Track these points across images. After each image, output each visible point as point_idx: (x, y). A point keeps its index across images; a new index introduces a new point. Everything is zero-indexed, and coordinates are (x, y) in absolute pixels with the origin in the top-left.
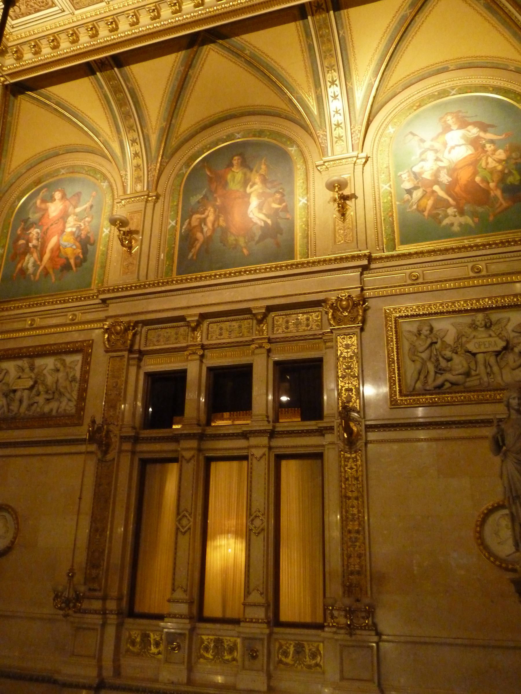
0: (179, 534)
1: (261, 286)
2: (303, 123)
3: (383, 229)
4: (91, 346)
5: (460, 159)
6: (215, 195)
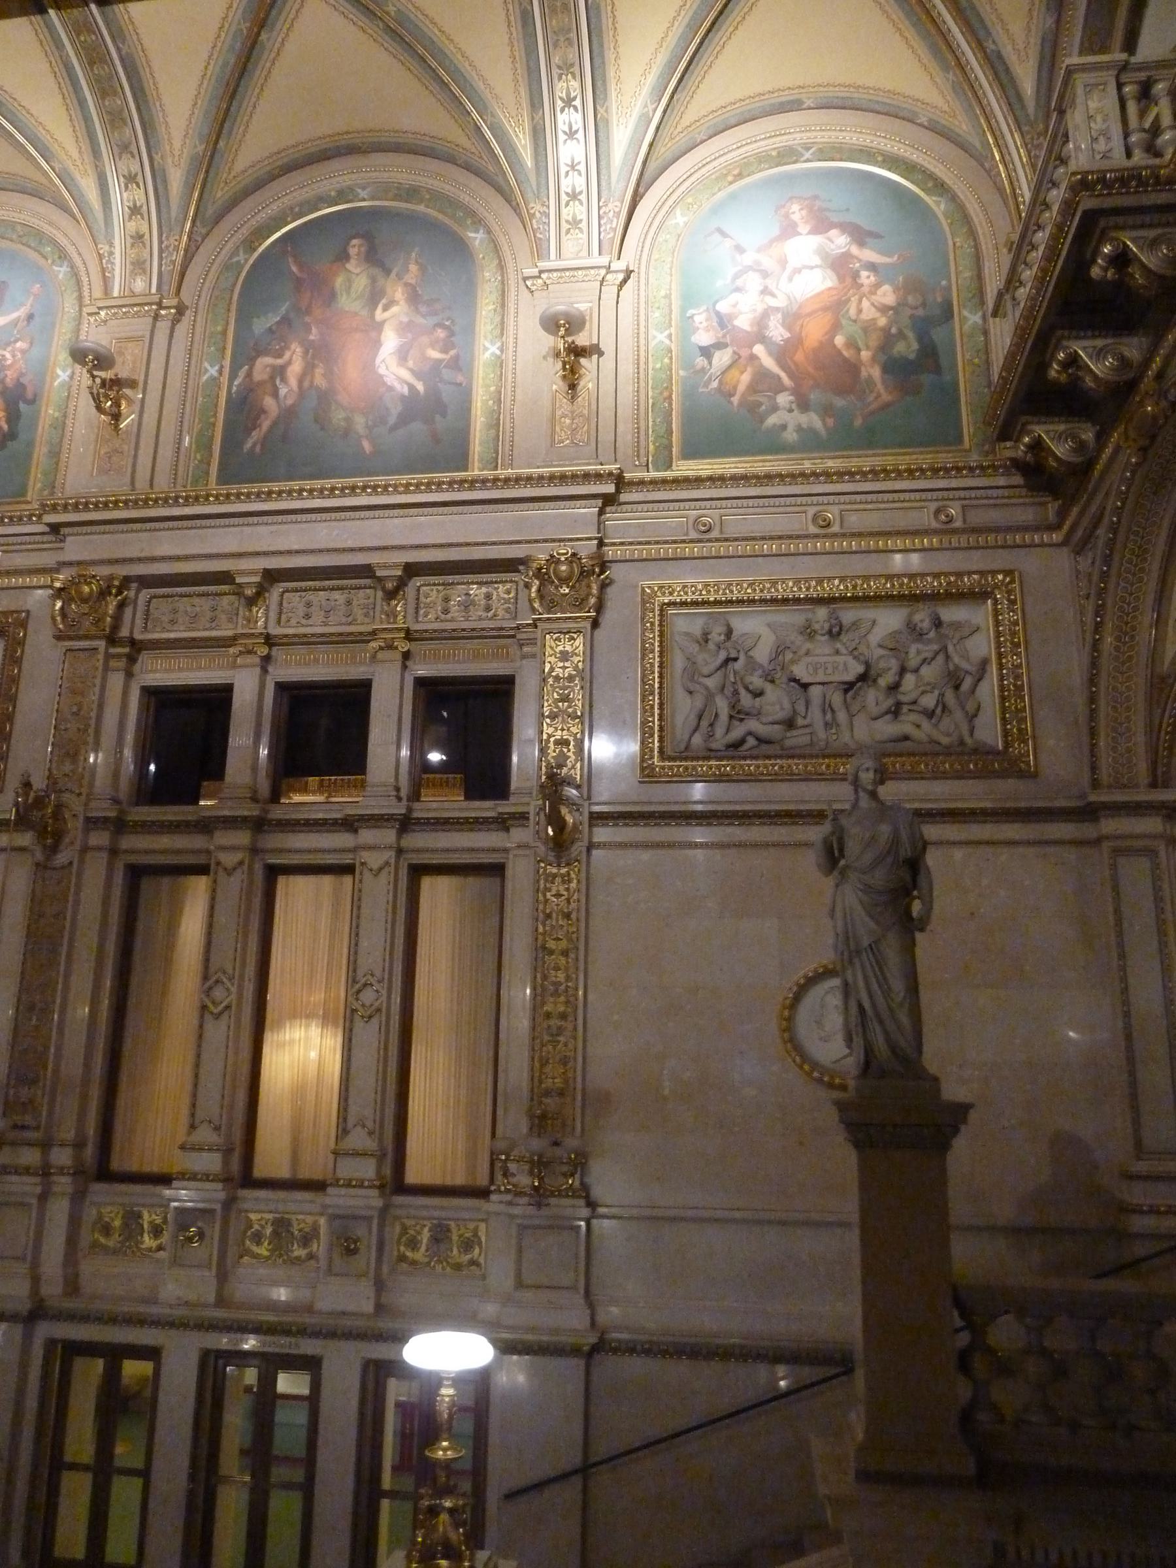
0: (207, 1016)
1: (396, 521)
2: (500, 179)
3: (651, 424)
4: (23, 624)
5: (809, 296)
6: (307, 319)
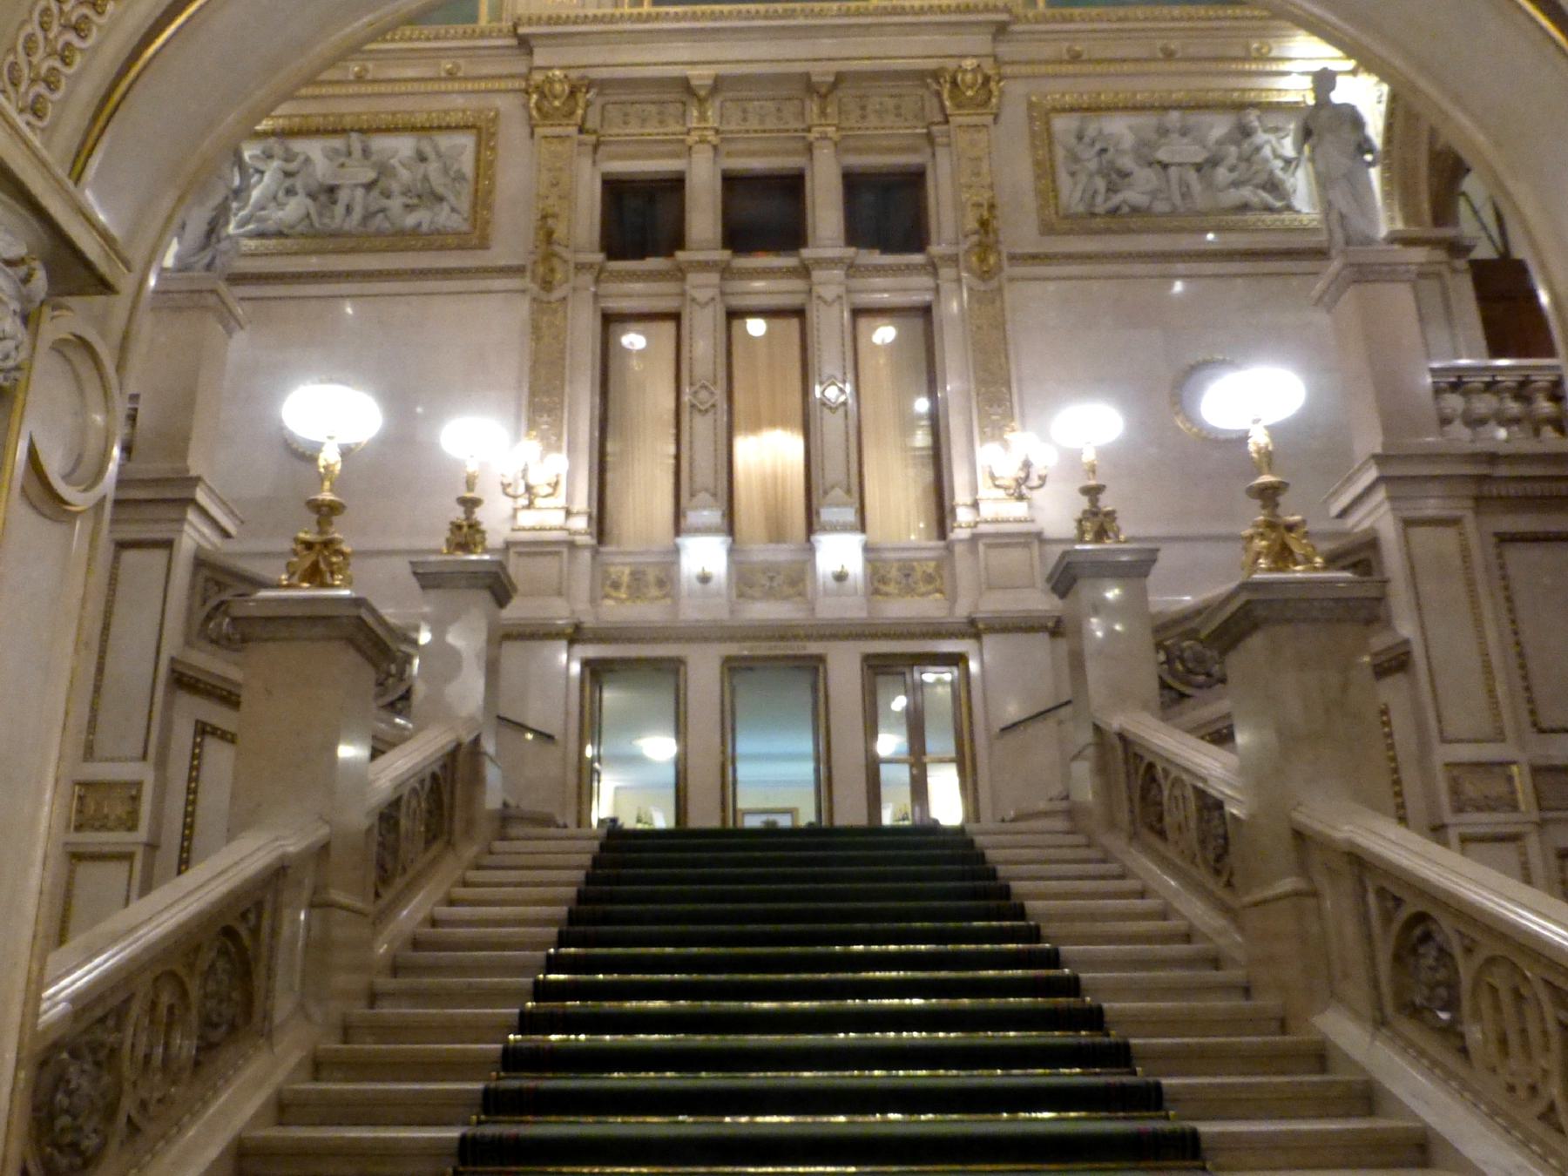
4: (494, 120)
